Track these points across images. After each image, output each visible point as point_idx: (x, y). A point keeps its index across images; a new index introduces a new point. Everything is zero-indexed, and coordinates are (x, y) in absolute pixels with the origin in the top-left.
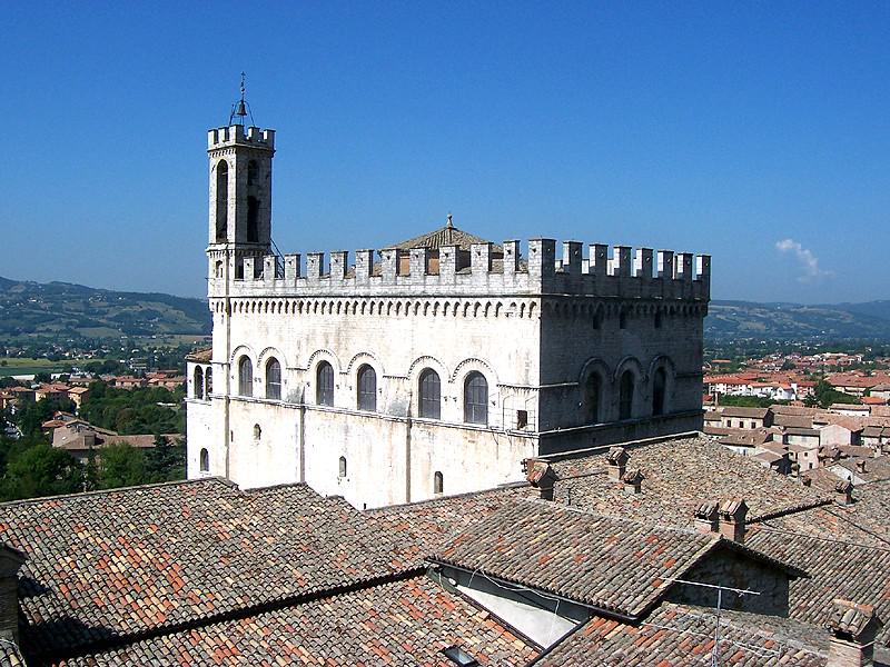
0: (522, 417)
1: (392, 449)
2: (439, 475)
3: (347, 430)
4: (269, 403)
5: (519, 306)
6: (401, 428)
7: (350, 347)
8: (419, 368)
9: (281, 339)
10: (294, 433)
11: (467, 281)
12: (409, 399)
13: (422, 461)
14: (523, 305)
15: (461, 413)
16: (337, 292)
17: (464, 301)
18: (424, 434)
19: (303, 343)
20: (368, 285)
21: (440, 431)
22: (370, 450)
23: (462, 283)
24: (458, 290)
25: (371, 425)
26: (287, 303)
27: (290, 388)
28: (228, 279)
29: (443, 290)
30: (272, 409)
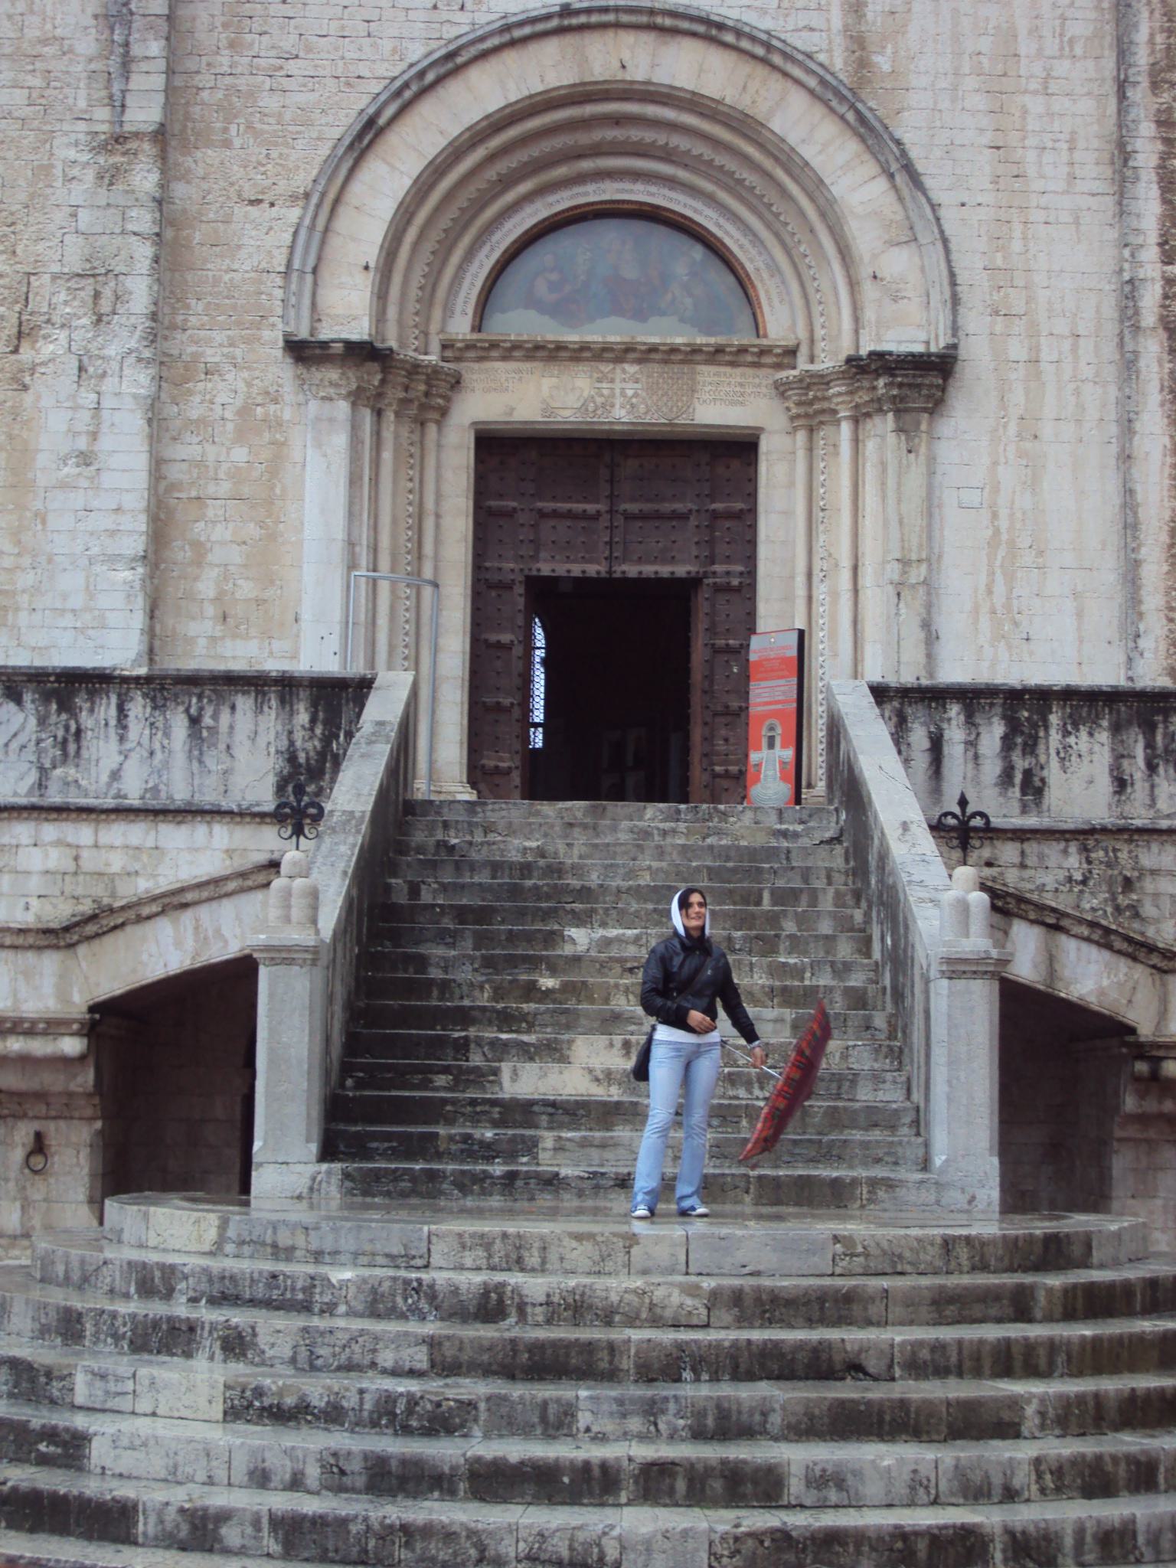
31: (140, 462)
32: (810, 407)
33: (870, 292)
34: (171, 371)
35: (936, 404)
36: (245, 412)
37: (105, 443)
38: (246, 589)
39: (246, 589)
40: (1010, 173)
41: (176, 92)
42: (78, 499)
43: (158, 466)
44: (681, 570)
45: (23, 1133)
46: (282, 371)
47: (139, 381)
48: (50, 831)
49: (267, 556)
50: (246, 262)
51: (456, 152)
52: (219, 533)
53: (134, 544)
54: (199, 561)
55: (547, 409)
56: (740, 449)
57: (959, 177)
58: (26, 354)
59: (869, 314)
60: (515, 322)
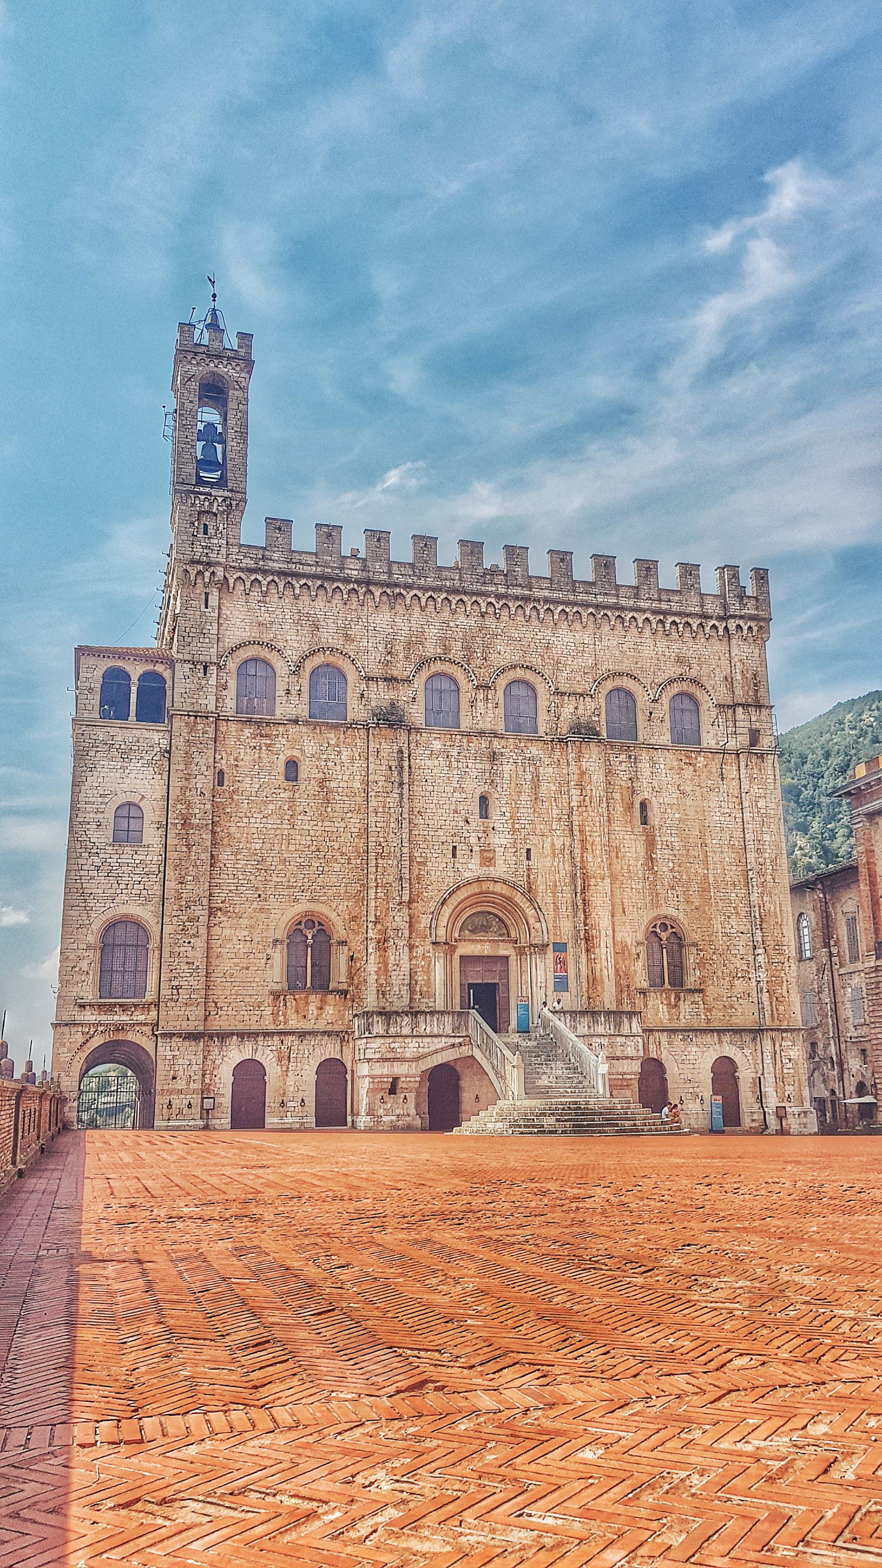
0: (754, 736)
1: (582, 774)
2: (643, 805)
3: (493, 757)
5: (745, 628)
7: (493, 657)
8: (609, 685)
9: (347, 638)
10: (393, 764)
14: (750, 628)
17: (670, 619)
18: (623, 757)
21: (644, 756)
23: (669, 601)
24: (664, 606)
25: (534, 750)
27: (373, 704)
29: (642, 604)
30: (332, 737)
32: (521, 952)
33: (532, 931)
34: (411, 947)
36: (423, 954)
37: (402, 962)
38: (425, 989)
39: (425, 989)
40: (556, 909)
42: (397, 973)
44: (495, 981)
45: (403, 1095)
46: (431, 947)
47: (406, 949)
48: (414, 1040)
50: (422, 925)
52: (420, 978)
54: (416, 984)
55: (473, 951)
57: (549, 910)
58: (386, 945)
59: (532, 935)
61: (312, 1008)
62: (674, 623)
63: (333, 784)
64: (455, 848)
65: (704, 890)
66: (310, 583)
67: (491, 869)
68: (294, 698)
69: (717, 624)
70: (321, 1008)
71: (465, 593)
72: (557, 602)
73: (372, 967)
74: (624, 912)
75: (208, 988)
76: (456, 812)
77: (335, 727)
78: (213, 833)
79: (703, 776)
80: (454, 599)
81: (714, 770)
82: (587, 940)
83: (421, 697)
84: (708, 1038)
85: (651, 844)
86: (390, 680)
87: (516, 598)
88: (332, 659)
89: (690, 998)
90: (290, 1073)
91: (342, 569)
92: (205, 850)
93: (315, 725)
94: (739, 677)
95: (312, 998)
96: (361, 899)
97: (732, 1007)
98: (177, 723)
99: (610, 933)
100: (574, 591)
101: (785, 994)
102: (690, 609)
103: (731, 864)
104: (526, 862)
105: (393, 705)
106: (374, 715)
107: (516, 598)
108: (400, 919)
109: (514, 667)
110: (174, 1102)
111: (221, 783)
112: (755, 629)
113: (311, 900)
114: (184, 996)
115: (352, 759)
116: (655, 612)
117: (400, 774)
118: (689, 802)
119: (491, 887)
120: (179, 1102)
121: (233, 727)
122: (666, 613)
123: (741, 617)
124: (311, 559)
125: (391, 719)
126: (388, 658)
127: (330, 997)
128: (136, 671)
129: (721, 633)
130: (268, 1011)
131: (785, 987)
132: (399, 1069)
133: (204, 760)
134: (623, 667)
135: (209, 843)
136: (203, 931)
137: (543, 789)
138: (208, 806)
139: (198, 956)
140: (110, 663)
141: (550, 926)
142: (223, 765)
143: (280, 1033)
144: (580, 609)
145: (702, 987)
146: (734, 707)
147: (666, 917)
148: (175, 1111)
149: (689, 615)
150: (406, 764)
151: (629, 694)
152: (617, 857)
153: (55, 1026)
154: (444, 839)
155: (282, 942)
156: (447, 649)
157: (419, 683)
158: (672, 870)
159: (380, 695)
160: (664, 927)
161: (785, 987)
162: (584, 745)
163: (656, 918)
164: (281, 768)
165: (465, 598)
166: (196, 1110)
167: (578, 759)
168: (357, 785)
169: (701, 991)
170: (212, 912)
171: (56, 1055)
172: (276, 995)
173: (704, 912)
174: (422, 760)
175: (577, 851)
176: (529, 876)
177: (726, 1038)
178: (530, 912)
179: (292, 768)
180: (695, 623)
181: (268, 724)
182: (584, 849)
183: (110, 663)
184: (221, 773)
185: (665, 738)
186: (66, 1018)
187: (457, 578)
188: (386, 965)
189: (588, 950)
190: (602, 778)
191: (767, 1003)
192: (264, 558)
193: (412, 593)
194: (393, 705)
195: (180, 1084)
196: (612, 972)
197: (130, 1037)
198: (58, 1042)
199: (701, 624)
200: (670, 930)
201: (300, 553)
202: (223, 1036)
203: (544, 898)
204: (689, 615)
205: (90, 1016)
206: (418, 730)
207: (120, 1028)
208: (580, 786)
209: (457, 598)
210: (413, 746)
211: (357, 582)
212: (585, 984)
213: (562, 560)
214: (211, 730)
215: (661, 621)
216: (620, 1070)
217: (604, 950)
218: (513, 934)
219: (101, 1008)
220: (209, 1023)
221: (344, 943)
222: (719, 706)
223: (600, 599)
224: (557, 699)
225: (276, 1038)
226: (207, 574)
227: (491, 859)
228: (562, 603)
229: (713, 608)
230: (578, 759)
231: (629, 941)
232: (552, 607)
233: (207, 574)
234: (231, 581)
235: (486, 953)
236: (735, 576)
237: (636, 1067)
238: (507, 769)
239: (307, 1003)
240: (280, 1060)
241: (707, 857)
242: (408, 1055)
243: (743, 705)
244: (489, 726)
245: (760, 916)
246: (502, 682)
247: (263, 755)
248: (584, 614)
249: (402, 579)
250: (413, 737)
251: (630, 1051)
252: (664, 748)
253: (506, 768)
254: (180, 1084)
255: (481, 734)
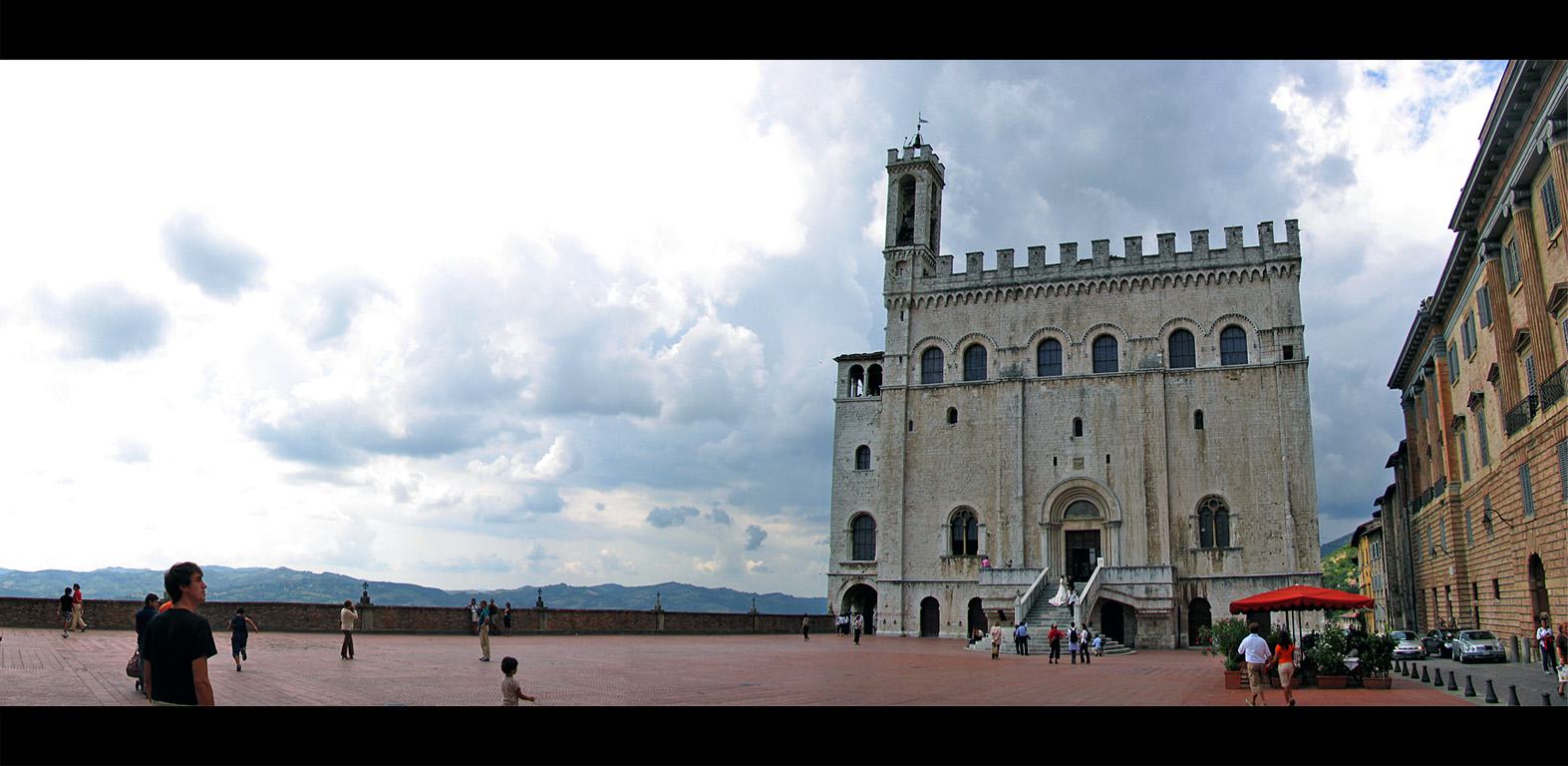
0: (1288, 352)
1: (1146, 397)
2: (1199, 415)
3: (1083, 393)
4: (969, 385)
5: (1279, 269)
6: (1156, 382)
7: (1084, 320)
8: (1171, 328)
9: (987, 325)
11: (1223, 255)
12: (1160, 355)
13: (1179, 402)
14: (1283, 268)
15: (1219, 360)
16: (1069, 275)
17: (1219, 272)
18: (1181, 380)
19: (1020, 327)
20: (1109, 267)
22: (1114, 406)
24: (1213, 263)
25: (1112, 385)
26: (999, 292)
28: (913, 278)
30: (975, 392)
31: (1022, 539)
34: (1025, 527)
35: (1119, 527)
38: (1035, 553)
41: (1024, 491)
43: (1024, 538)
46: (1039, 526)
47: (1021, 530)
49: (1038, 549)
50: (1034, 512)
51: (1059, 497)
53: (1022, 548)
56: (1099, 531)
60: (1070, 517)
61: (965, 566)
62: (1222, 274)
63: (976, 423)
64: (1055, 459)
65: (1245, 475)
66: (962, 293)
67: (1081, 471)
68: (953, 369)
69: (1257, 268)
70: (970, 567)
71: (1064, 280)
72: (1129, 275)
73: (999, 541)
74: (1180, 494)
75: (904, 554)
76: (1056, 433)
77: (977, 386)
78: (906, 461)
79: (1246, 388)
80: (1056, 286)
81: (1255, 382)
82: (1148, 516)
83: (1034, 357)
84: (1245, 583)
85: (1203, 442)
86: (1014, 350)
87: (1099, 277)
88: (977, 341)
89: (1231, 554)
90: (953, 606)
91: (981, 279)
92: (900, 471)
93: (965, 386)
94: (1275, 307)
95: (965, 560)
96: (993, 496)
97: (1265, 559)
98: (884, 395)
99: (1167, 510)
100: (1143, 264)
101: (1307, 547)
102: (1232, 263)
103: (1266, 452)
104: (1106, 465)
105: (1014, 366)
106: (1001, 373)
107: (1099, 277)
108: (1016, 508)
109: (1098, 327)
110: (887, 621)
111: (911, 429)
112: (1288, 268)
113: (964, 499)
114: (890, 559)
115: (988, 405)
116: (1205, 269)
117: (1017, 411)
118: (1234, 408)
119: (1081, 483)
120: (890, 620)
121: (917, 393)
122: (1215, 268)
123: (1275, 261)
124: (963, 278)
125: (1014, 376)
126: (1013, 334)
127: (976, 560)
128: (866, 366)
129: (1261, 275)
130: (940, 568)
131: (1307, 543)
132: (1003, 605)
133: (899, 414)
134: (1184, 315)
135: (902, 467)
136: (900, 521)
137: (1119, 413)
138: (902, 445)
139: (899, 535)
140: (853, 364)
141: (1124, 507)
142: (912, 416)
143: (946, 582)
144: (1147, 276)
145: (1241, 546)
146: (1272, 331)
147: (1214, 496)
148: (887, 624)
149: (1233, 266)
150: (1020, 404)
151: (1188, 333)
152: (1175, 455)
153: (829, 575)
154: (1048, 453)
155: (947, 526)
156: (1052, 321)
157: (1033, 349)
158: (1219, 461)
159: (1006, 362)
160: (1213, 503)
161: (1307, 543)
162: (1148, 376)
163: (1206, 498)
164: (945, 414)
165: (1063, 284)
166: (899, 625)
167: (1143, 387)
168: (991, 421)
169: (1239, 549)
170: (905, 510)
171: (830, 591)
172: (943, 559)
173: (1244, 490)
174: (1034, 401)
175: (1143, 453)
176: (1108, 474)
177: (1260, 582)
178: (1108, 499)
179: (953, 416)
180: (1239, 271)
181: (938, 389)
182: (1147, 451)
183: (853, 364)
184: (911, 423)
185: (1216, 362)
186: (835, 572)
187: (1057, 270)
188: (1008, 538)
189: (1148, 524)
190: (1162, 399)
191: (1292, 556)
192: (935, 283)
193: (1027, 287)
194: (1014, 366)
195: (889, 610)
196: (1167, 538)
197: (866, 582)
198: (831, 585)
199: (1244, 272)
200: (1218, 505)
201: (956, 275)
202: (914, 583)
203: (1119, 486)
204: (1233, 266)
205: (845, 571)
206: (1030, 381)
207: (860, 577)
208: (1144, 406)
209: (1058, 284)
210: (1027, 392)
211: (992, 287)
212: (1146, 547)
213: (1134, 244)
214: (903, 397)
215: (1211, 275)
216: (1156, 607)
217: (1161, 523)
218: (1102, 515)
219: (852, 566)
220: (906, 575)
221: (982, 525)
222: (1261, 332)
223: (1162, 266)
224: (1130, 344)
225: (944, 585)
226: (901, 300)
227: (1083, 463)
228: (1134, 274)
229: (1255, 258)
230: (1143, 387)
231: (1183, 515)
232: (1126, 279)
233: (901, 300)
234: (916, 302)
235: (1082, 529)
236: (1270, 230)
237: (1169, 604)
238: (1091, 399)
239: (962, 564)
240: (946, 598)
241: (1248, 448)
242: (1006, 597)
243: (1278, 329)
244: (1081, 371)
245: (1290, 491)
246: (1091, 339)
247: (934, 409)
248: (1151, 279)
249: (1020, 280)
250: (1027, 385)
251: (1162, 593)
252: (1216, 370)
253: (1092, 399)
254: (889, 610)
255: (1074, 378)
